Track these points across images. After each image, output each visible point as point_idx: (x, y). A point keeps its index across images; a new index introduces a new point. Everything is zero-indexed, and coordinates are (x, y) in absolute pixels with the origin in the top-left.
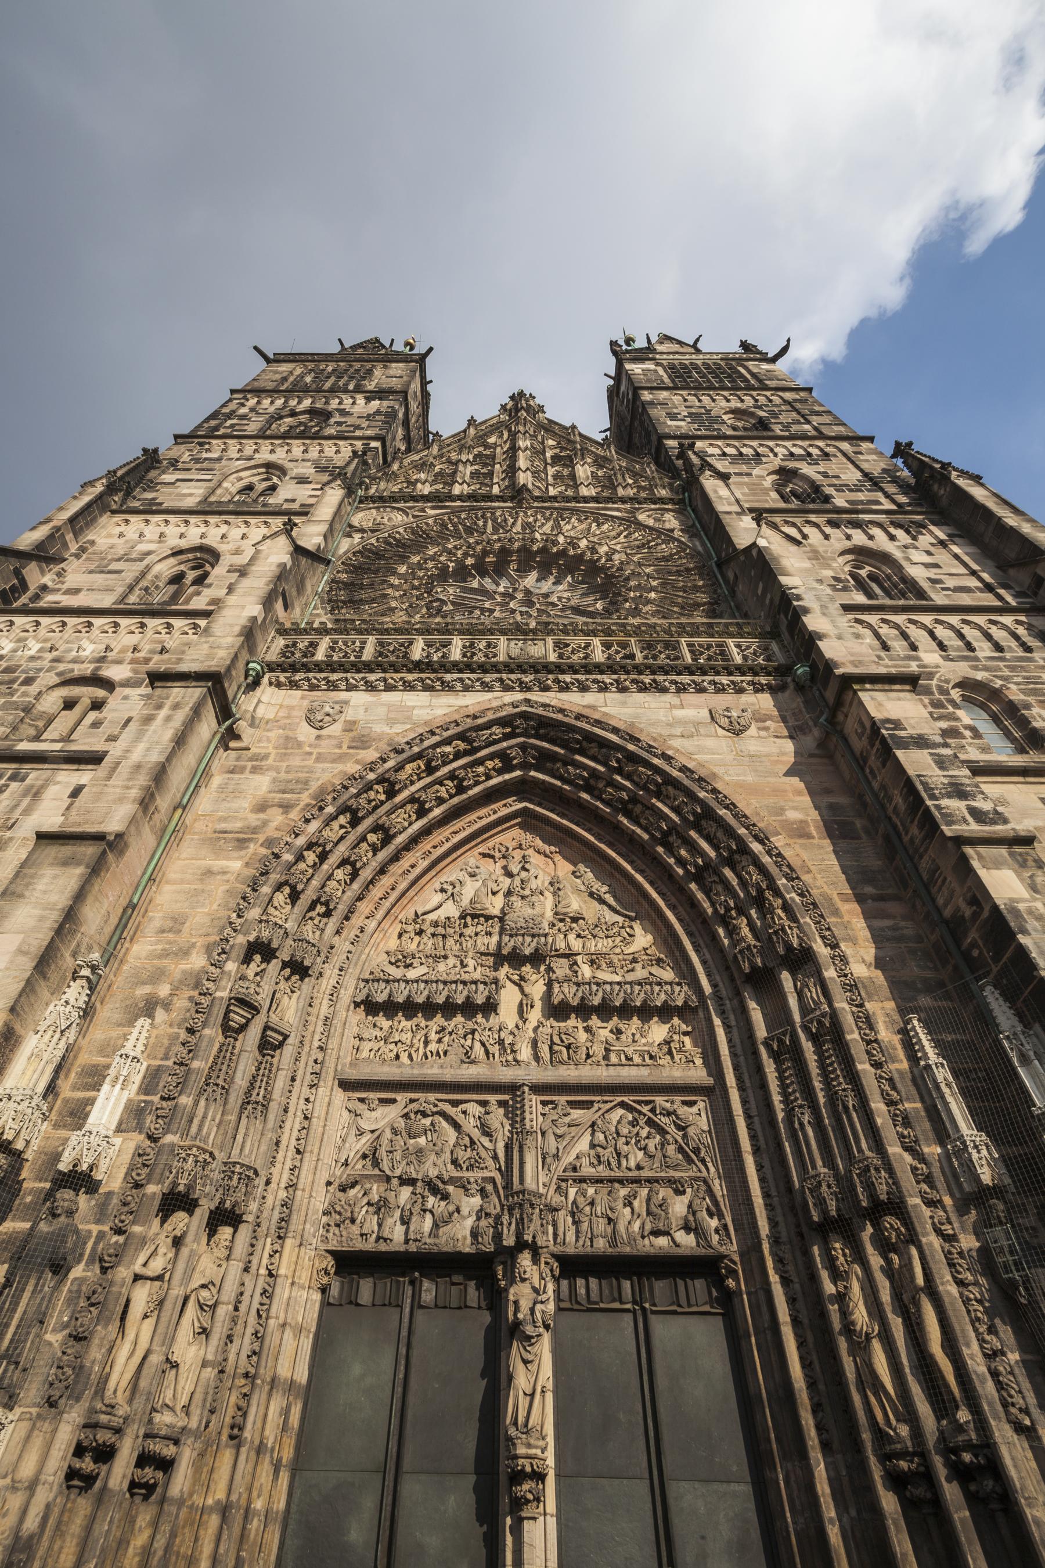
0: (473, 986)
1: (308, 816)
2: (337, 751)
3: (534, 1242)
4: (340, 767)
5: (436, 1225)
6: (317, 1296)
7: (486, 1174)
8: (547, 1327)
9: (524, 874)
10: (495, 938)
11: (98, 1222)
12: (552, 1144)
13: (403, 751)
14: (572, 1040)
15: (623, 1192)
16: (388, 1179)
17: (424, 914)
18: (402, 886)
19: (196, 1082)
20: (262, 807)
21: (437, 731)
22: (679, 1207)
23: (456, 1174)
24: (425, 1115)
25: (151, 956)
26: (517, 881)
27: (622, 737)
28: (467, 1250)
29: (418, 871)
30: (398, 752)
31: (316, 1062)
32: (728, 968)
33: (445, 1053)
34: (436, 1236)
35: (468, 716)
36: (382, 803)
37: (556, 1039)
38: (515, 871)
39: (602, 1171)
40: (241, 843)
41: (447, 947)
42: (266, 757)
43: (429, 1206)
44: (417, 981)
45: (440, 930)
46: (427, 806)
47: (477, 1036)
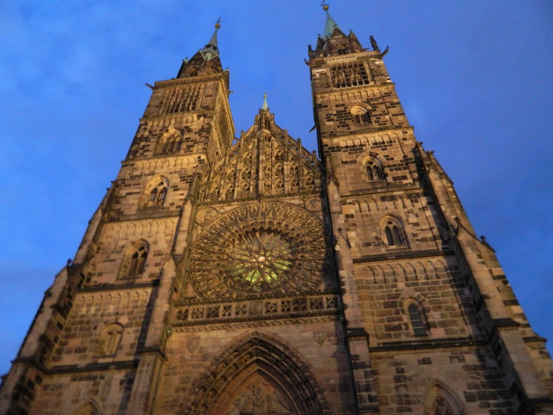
2: (198, 363)
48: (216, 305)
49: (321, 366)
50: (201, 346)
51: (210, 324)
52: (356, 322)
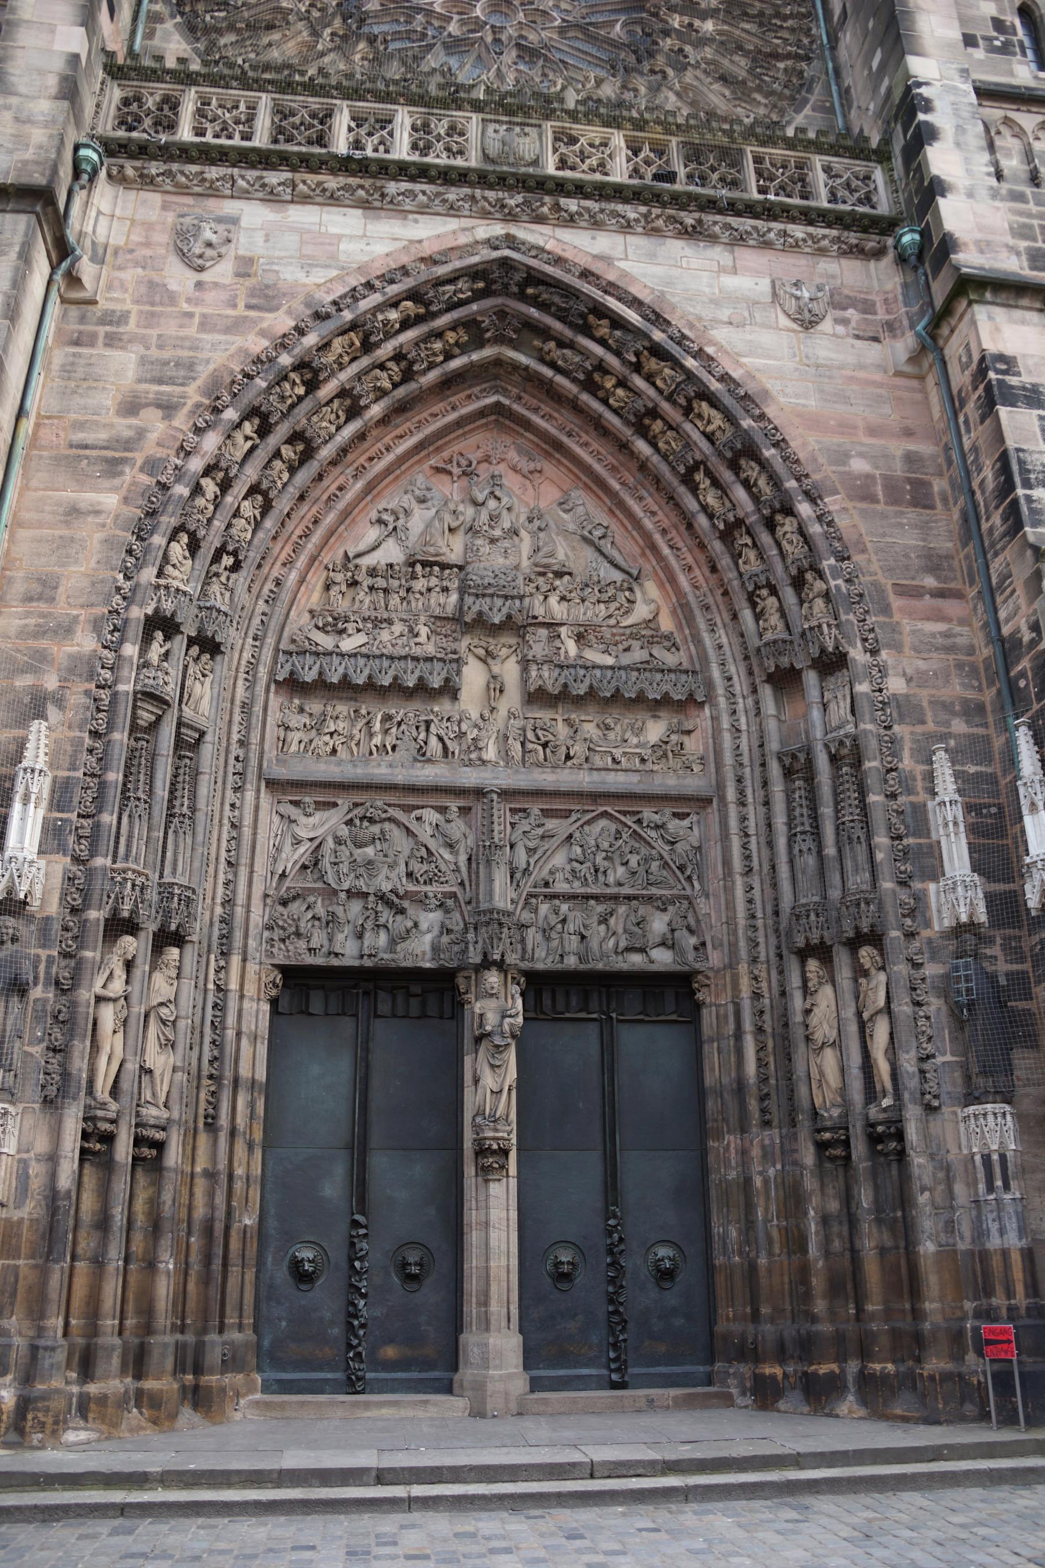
0: (428, 665)
1: (201, 424)
2: (230, 312)
3: (502, 960)
4: (237, 341)
5: (393, 942)
6: (266, 1007)
7: (447, 889)
8: (513, 1036)
9: (492, 504)
10: (454, 597)
11: (44, 946)
12: (521, 858)
13: (328, 316)
14: (551, 737)
15: (600, 908)
16: (335, 892)
17: (358, 556)
18: (330, 519)
19: (114, 796)
20: (131, 407)
21: (377, 284)
22: (659, 924)
23: (411, 888)
24: (371, 821)
25: (23, 633)
26: (484, 517)
27: (645, 317)
28: (428, 965)
29: (349, 496)
30: (319, 316)
31: (237, 759)
32: (746, 658)
33: (394, 748)
34: (393, 951)
35: (422, 260)
36: (300, 399)
37: (530, 735)
38: (480, 498)
39: (577, 888)
40: (113, 467)
41: (391, 607)
42: (123, 318)
43: (382, 921)
44: (355, 655)
45: (381, 583)
46: (362, 403)
47: (433, 729)
48: (315, 102)
49: (812, 403)
50: (241, 252)
51: (294, 169)
52: (983, 246)
